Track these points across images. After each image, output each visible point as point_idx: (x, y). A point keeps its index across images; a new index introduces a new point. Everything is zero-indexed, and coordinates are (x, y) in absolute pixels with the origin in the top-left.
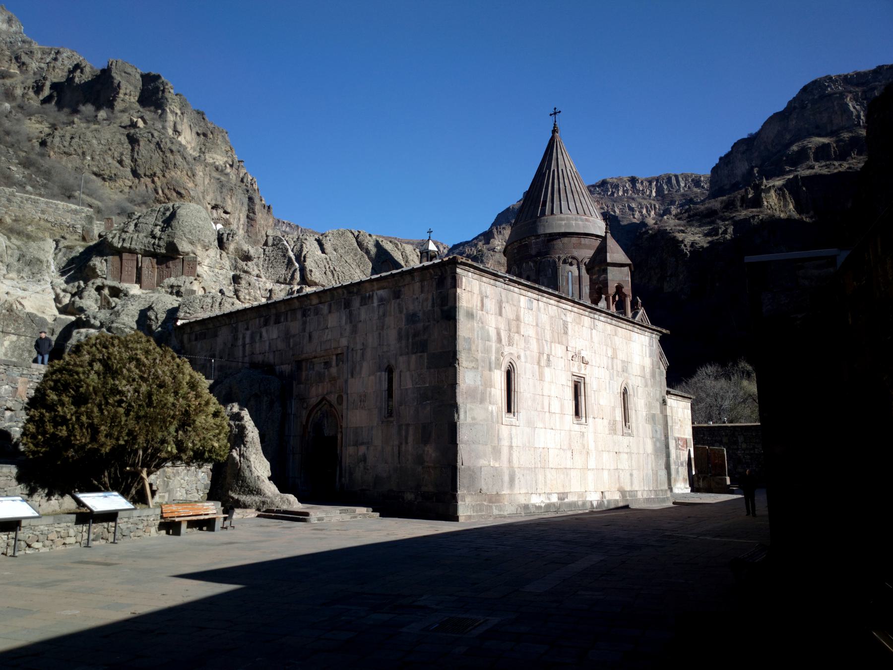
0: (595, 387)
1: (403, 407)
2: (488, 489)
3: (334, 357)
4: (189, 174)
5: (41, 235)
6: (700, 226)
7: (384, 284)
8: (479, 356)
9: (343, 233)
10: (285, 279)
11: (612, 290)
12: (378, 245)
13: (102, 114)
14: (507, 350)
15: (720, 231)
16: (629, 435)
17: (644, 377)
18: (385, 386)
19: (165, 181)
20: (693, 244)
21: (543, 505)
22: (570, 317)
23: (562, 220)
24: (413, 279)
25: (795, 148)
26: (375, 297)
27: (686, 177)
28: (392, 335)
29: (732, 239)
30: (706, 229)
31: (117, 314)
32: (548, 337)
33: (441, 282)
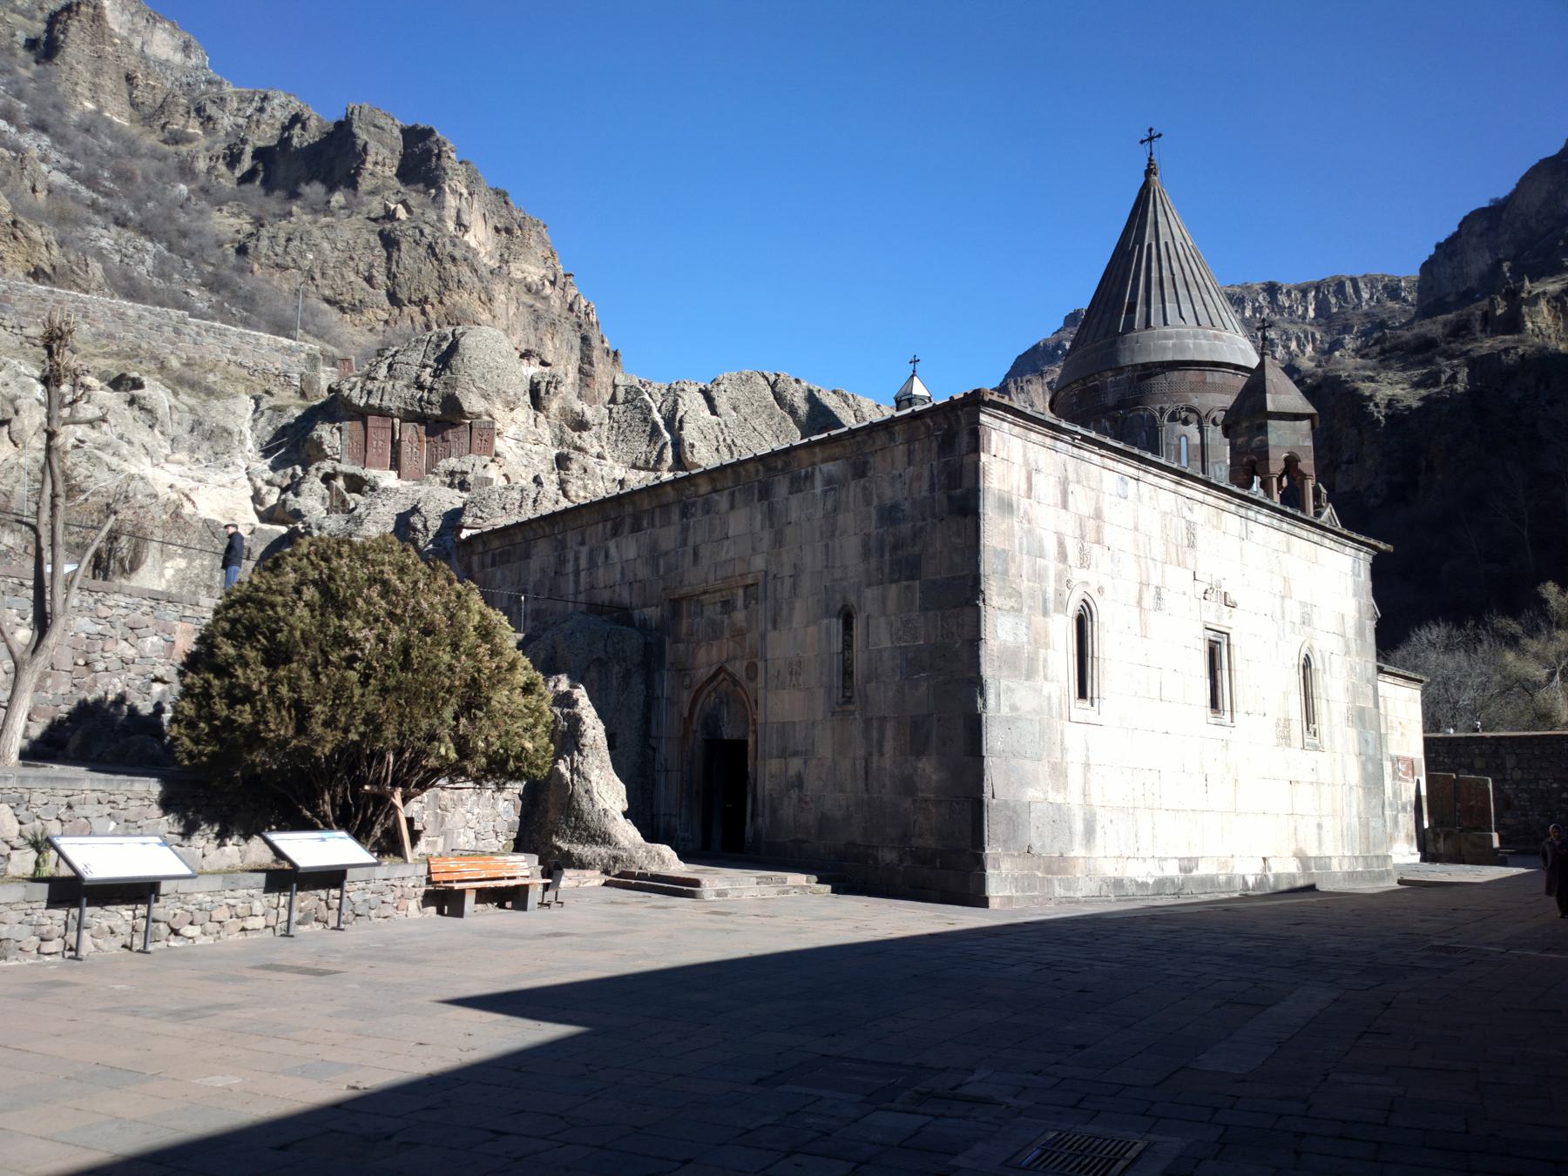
1: (873, 684)
2: (1043, 847)
3: (741, 592)
4: (483, 297)
5: (230, 389)
6: (1404, 369)
8: (1025, 586)
9: (749, 378)
10: (647, 462)
11: (1276, 465)
12: (811, 398)
13: (338, 198)
14: (1078, 575)
15: (1444, 378)
16: (1316, 748)
17: (1343, 636)
18: (837, 645)
19: (443, 310)
20: (1391, 403)
21: (1151, 881)
22: (1201, 514)
24: (892, 438)
27: (1372, 281)
28: (850, 548)
29: (1467, 394)
30: (1416, 374)
31: (359, 521)
32: (1157, 549)
33: (947, 442)
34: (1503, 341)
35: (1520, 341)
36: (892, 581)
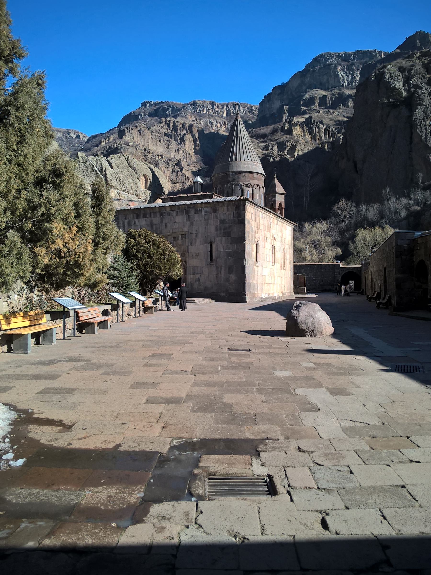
0: (277, 250)
1: (219, 259)
3: (180, 236)
7: (208, 205)
8: (251, 238)
11: (278, 205)
14: (257, 236)
15: (270, 148)
16: (285, 270)
18: (209, 249)
22: (272, 220)
23: (245, 164)
24: (224, 205)
25: (307, 96)
26: (203, 211)
27: (244, 106)
28: (212, 229)
32: (266, 229)
33: (238, 207)
34: (287, 138)
35: (291, 138)
36: (223, 237)
